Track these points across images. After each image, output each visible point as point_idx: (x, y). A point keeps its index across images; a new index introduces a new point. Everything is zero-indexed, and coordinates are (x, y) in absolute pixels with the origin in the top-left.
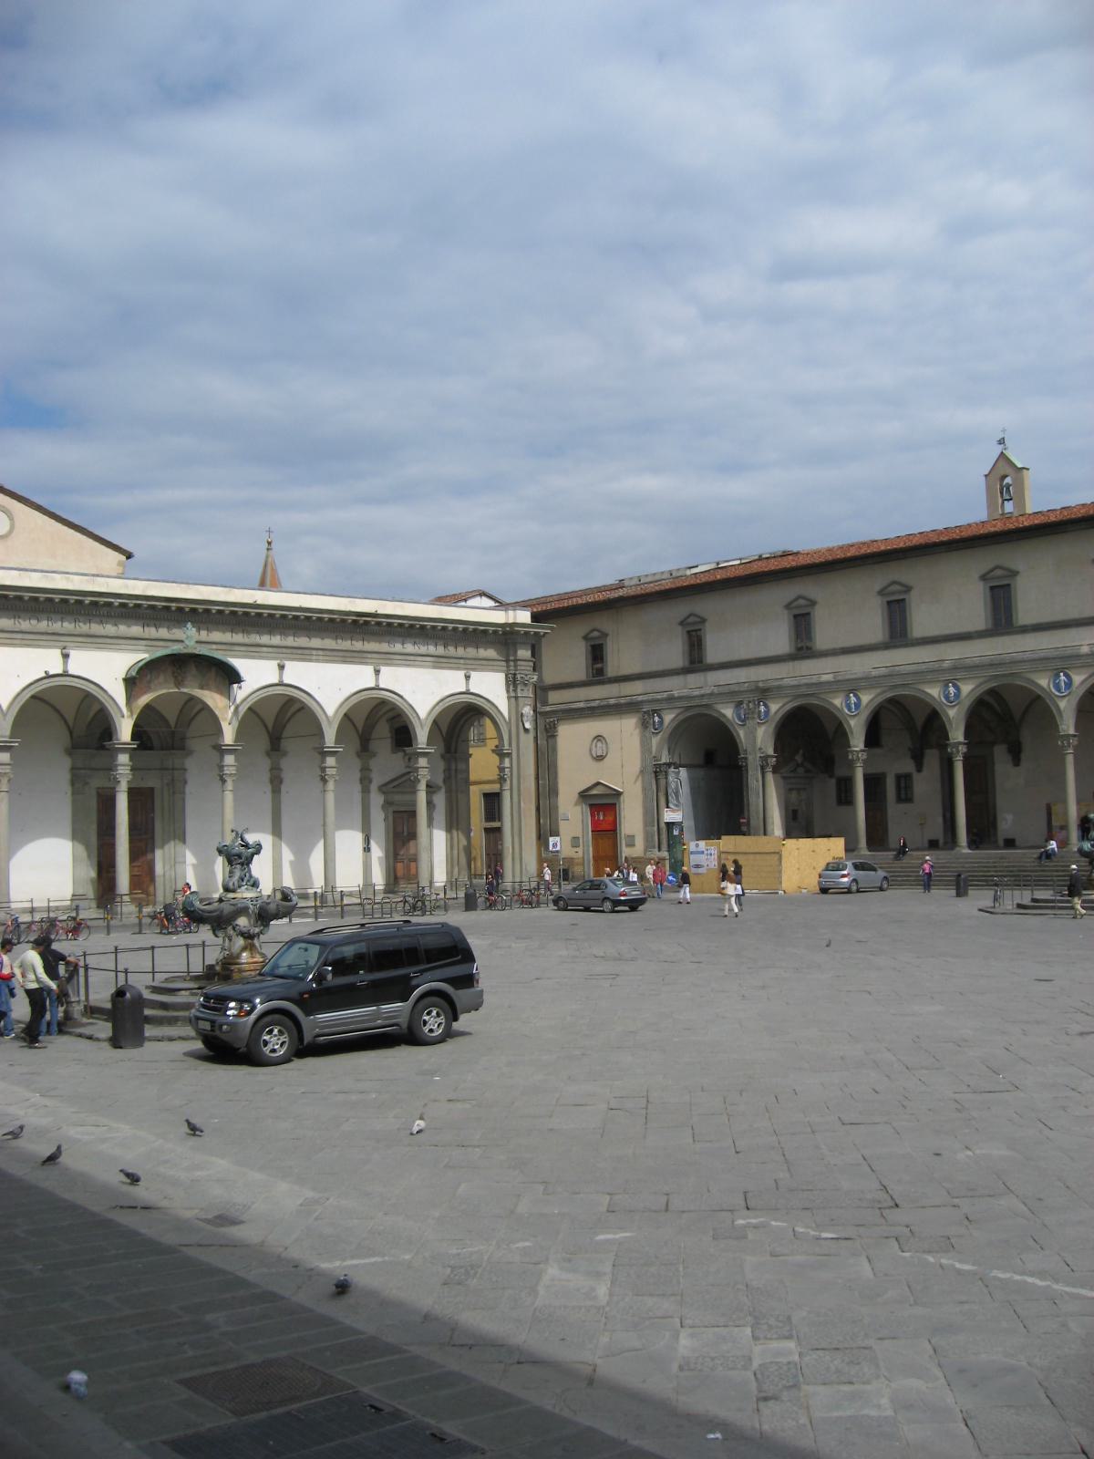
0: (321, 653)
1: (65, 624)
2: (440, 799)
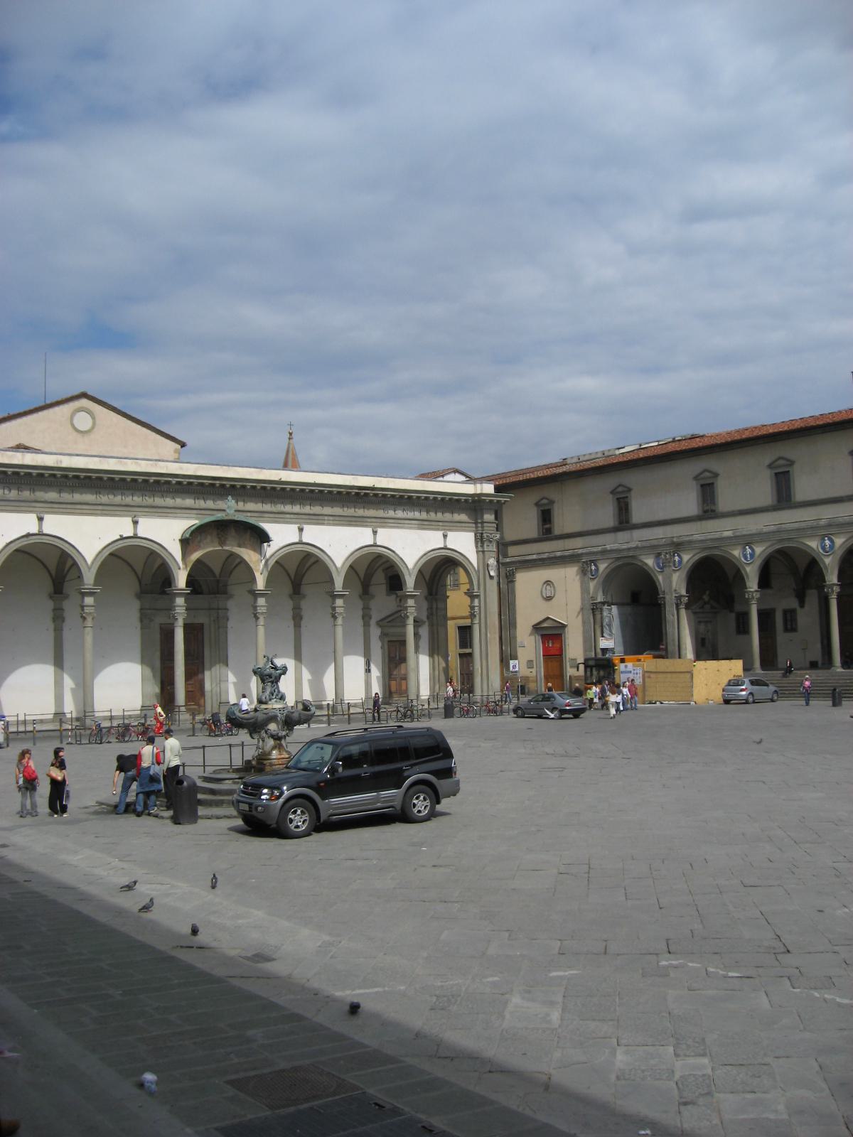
0: (331, 518)
1: (135, 498)
2: (424, 631)
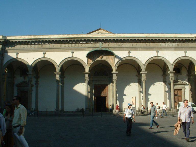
0: (140, 48)
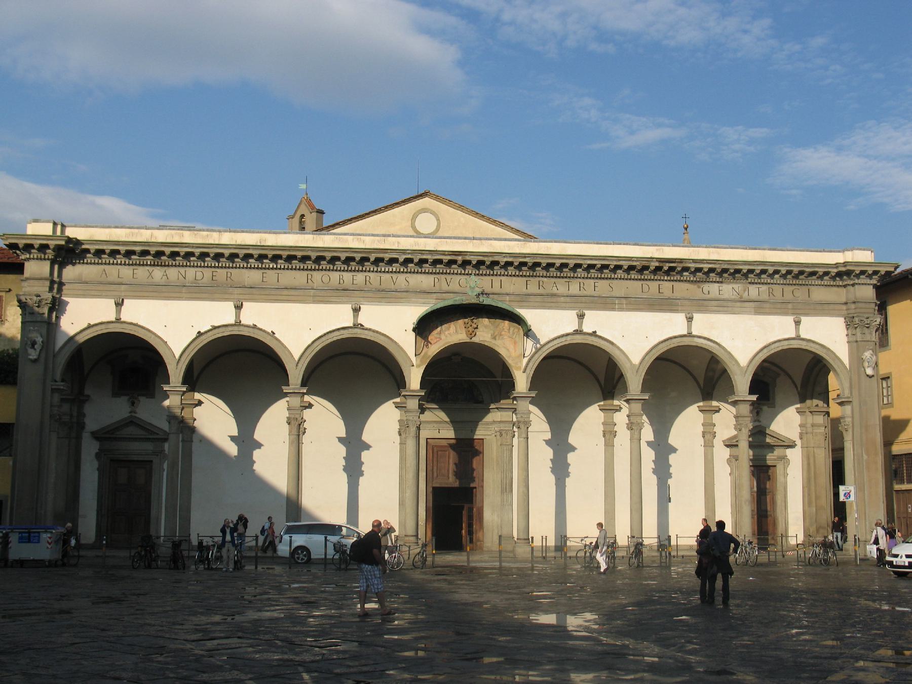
0: (624, 301)
